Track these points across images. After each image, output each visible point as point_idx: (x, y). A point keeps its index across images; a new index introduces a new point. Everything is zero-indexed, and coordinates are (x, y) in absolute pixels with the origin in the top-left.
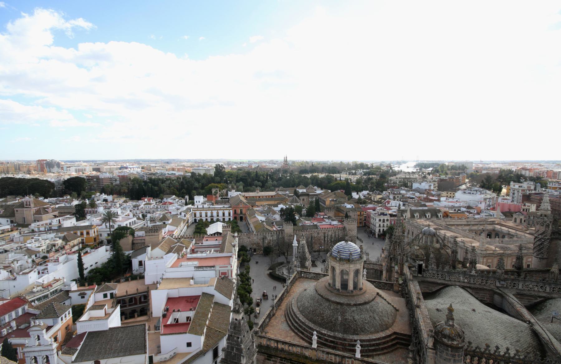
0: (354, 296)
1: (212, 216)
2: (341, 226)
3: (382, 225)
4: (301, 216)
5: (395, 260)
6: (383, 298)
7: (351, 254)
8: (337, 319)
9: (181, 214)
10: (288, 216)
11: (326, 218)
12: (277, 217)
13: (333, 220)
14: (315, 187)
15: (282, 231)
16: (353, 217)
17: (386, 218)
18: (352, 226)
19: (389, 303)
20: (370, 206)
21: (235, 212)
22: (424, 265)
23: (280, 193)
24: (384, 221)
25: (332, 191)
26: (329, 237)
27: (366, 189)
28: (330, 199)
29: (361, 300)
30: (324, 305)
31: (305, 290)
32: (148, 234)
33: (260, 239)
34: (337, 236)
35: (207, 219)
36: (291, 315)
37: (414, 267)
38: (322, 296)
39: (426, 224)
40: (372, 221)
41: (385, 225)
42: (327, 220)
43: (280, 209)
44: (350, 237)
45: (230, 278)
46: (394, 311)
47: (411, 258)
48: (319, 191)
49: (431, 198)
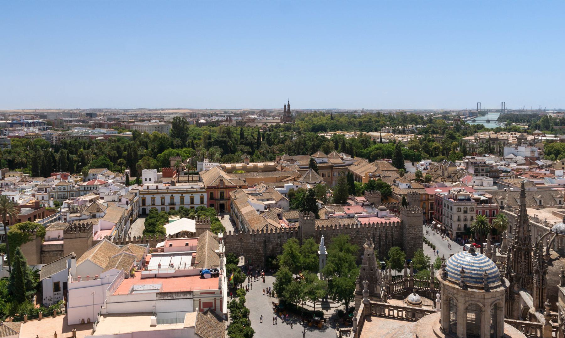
1: (172, 203)
2: (395, 220)
3: (462, 217)
4: (325, 202)
9: (120, 200)
10: (306, 203)
11: (367, 206)
17: (469, 205)
21: (211, 197)
24: (465, 212)
32: (69, 236)
33: (260, 243)
35: (163, 209)
40: (445, 210)
41: (469, 217)
42: (370, 210)
44: (412, 239)
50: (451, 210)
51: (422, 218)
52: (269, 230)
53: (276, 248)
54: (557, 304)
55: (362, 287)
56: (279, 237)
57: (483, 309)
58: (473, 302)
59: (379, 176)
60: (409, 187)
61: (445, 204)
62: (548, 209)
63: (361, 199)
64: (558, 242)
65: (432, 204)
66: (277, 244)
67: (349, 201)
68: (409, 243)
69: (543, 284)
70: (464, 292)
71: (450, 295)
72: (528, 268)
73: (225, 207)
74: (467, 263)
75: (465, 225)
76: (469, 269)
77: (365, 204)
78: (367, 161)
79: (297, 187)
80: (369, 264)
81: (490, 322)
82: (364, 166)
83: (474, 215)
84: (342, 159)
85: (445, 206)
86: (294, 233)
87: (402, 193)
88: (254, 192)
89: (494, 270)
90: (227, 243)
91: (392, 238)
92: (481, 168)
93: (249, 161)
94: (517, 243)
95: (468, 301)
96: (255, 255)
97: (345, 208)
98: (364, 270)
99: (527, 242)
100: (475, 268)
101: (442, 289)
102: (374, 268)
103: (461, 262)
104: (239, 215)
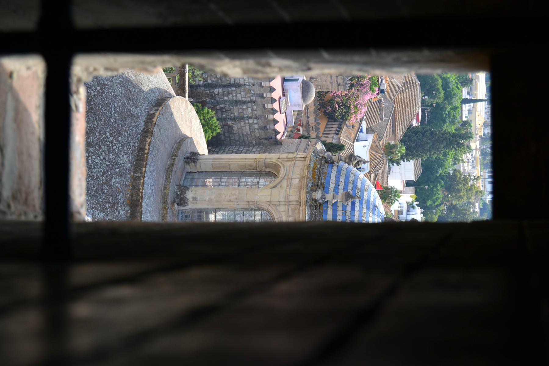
2: (280, 127)
30: (117, 147)
38: (147, 132)
70: (299, 203)
91: (234, 119)
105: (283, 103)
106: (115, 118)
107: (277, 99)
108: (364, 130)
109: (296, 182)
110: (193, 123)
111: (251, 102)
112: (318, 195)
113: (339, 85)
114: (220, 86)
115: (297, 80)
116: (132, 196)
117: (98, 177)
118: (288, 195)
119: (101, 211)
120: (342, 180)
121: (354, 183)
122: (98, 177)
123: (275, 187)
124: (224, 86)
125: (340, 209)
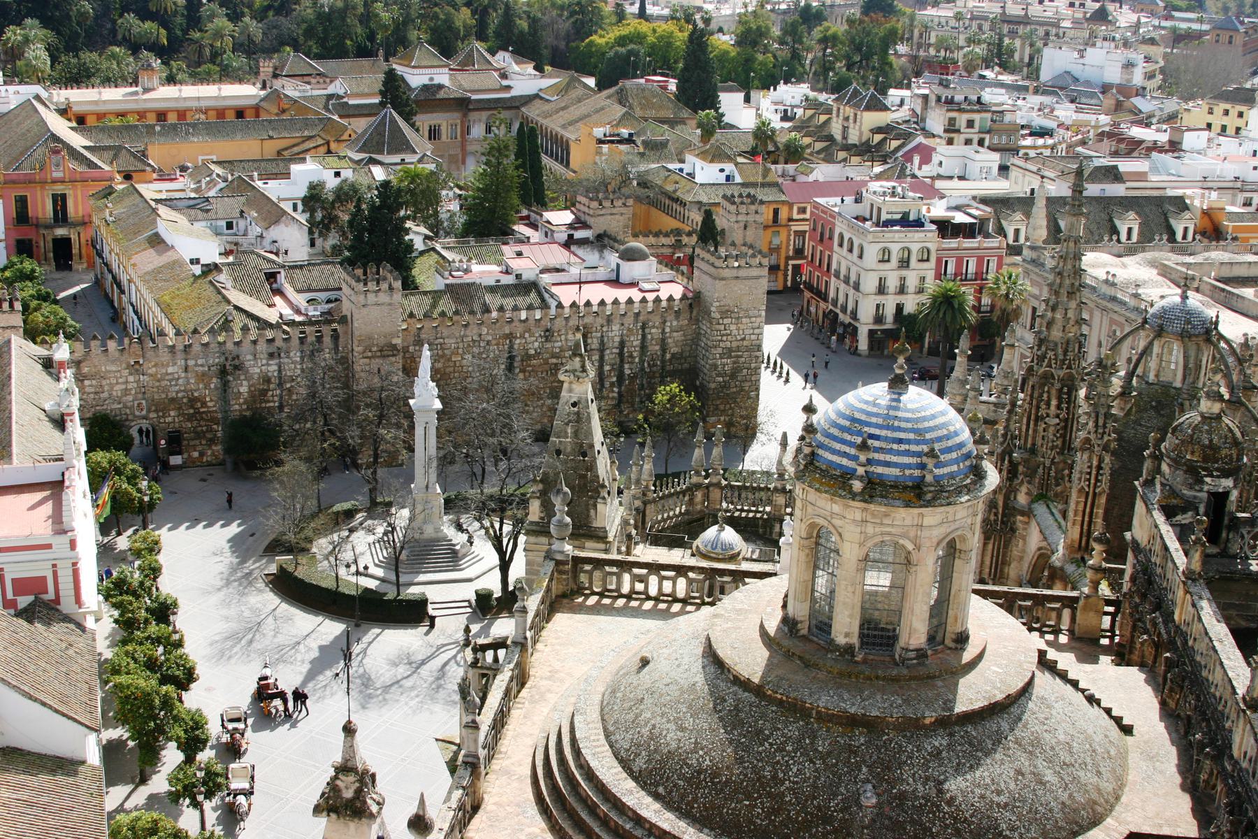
0: (931, 677)
3: (892, 284)
4: (436, 229)
5: (1031, 474)
6: (1063, 676)
7: (932, 454)
8: (856, 799)
11: (583, 242)
12: (293, 239)
13: (631, 256)
14: (503, 59)
15: (334, 319)
16: (737, 235)
17: (918, 240)
18: (739, 288)
19: (1091, 700)
20: (822, 172)
22: (1234, 495)
23: (292, 89)
24: (905, 263)
25: (601, 86)
26: (611, 355)
27: (800, 80)
28: (599, 132)
29: (972, 693)
30: (777, 738)
31: (645, 662)
33: (202, 377)
34: (655, 348)
36: (584, 800)
37: (1190, 506)
39: (1130, 273)
40: (840, 258)
41: (912, 283)
42: (591, 256)
43: (302, 192)
44: (728, 352)
45: (67, 605)
46: (1115, 731)
47: (1176, 463)
48: (524, 79)
49: (1137, 132)
50: (861, 257)
51: (764, 285)
52: (237, 326)
53: (264, 393)
54: (1128, 535)
55: (548, 508)
56: (271, 355)
57: (914, 557)
58: (887, 538)
59: (629, 140)
60: (728, 178)
61: (841, 236)
62: (1149, 255)
63: (560, 218)
64: (1160, 356)
65: (801, 234)
66: (268, 380)
67: (521, 229)
68: (715, 366)
69: (1097, 480)
71: (825, 523)
72: (1063, 436)
73: (75, 251)
74: (880, 421)
75: (899, 308)
76: (886, 439)
77: (579, 234)
78: (591, 82)
79: (337, 174)
80: (576, 434)
81: (929, 594)
82: (579, 100)
83: (930, 275)
84: (504, 76)
85: (841, 245)
86: (327, 340)
87: (705, 199)
88: (177, 195)
89: (958, 440)
90: (85, 377)
91: (664, 350)
92: (962, 119)
93: (156, 81)
94: (1041, 358)
95: (874, 535)
96: (190, 418)
97: (508, 251)
98: (558, 452)
99: (1070, 355)
100: (902, 435)
101: (798, 504)
102: (592, 446)
103: (863, 417)
104: (124, 279)
105: (646, 286)
106: (740, 735)
107: (642, 295)
108: (679, 166)
109: (836, 508)
110: (740, 606)
111: (643, 328)
112: (857, 485)
113: (624, 204)
114: (621, 367)
115: (618, 265)
116: (841, 724)
117: (816, 770)
118: (854, 520)
119: (860, 770)
120: (838, 446)
121: (843, 429)
122: (816, 770)
123: (840, 535)
124: (622, 361)
125: (876, 456)
